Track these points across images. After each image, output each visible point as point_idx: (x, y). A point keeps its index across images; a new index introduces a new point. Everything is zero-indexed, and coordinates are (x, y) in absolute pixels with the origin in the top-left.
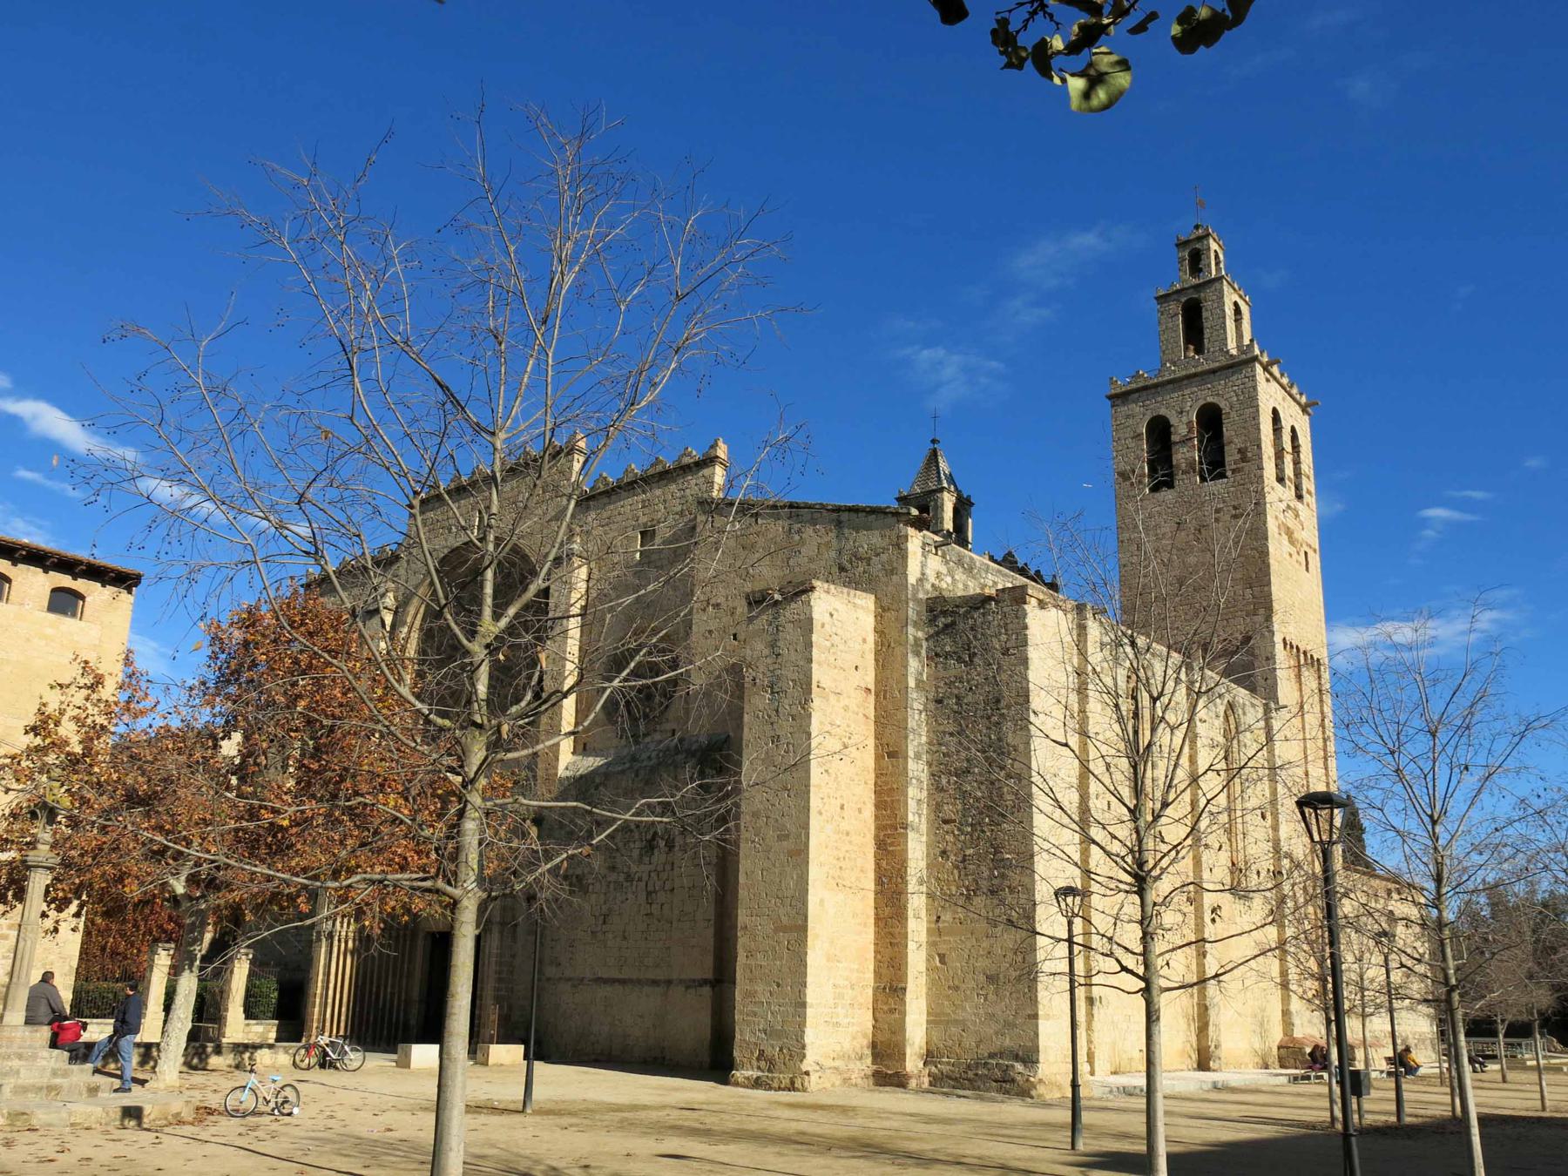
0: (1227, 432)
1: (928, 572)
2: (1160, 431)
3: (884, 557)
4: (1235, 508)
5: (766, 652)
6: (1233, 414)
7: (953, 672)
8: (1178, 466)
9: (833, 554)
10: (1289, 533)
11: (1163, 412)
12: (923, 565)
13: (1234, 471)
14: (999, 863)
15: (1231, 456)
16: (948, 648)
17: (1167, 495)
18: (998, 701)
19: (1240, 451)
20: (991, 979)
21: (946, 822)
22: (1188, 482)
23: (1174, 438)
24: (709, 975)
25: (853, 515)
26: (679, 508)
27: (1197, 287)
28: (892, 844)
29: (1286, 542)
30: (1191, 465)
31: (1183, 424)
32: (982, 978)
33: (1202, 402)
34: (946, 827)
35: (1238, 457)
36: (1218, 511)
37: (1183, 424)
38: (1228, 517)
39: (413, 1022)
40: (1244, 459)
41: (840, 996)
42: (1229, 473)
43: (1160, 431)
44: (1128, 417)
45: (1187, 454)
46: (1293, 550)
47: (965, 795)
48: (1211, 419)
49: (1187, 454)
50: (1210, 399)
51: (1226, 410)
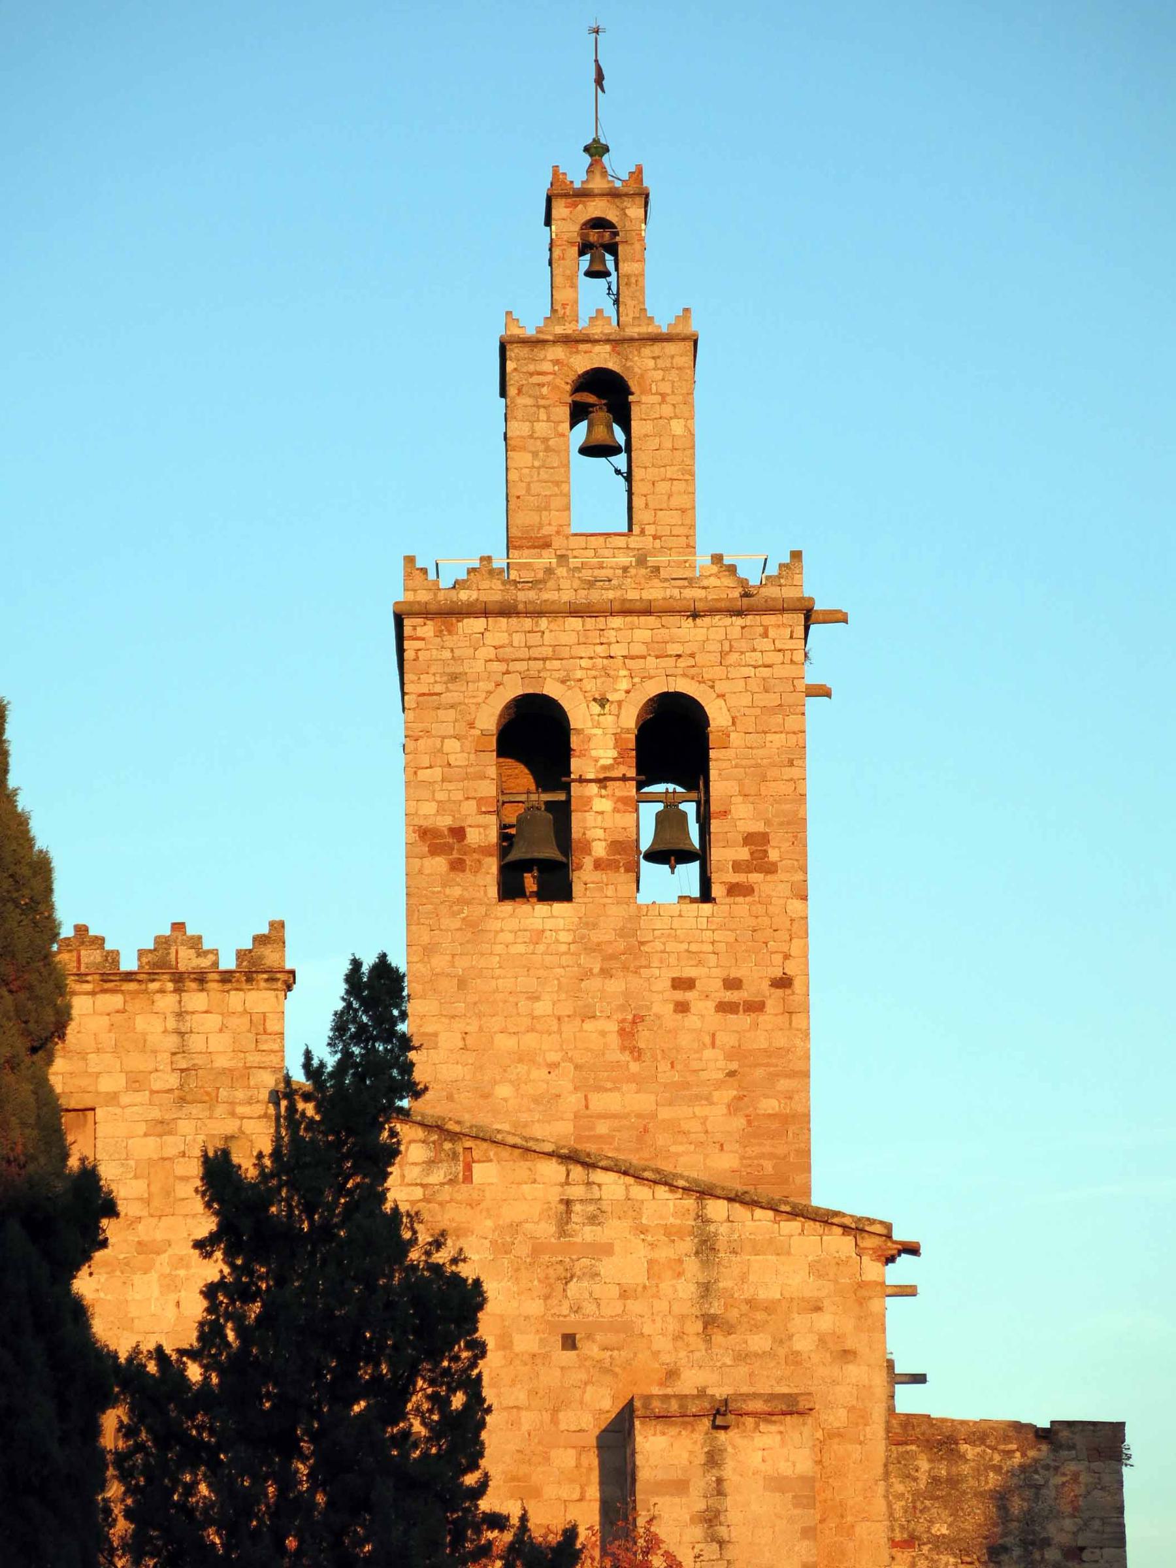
3: (825, 1322)
4: (732, 984)
5: (698, 1532)
8: (587, 848)
11: (552, 690)
16: (940, 1529)
19: (749, 839)
23: (575, 764)
25: (738, 1209)
26: (173, 1080)
31: (601, 739)
35: (743, 854)
36: (683, 984)
38: (711, 1005)
40: (760, 863)
43: (535, 734)
44: (454, 678)
48: (673, 741)
51: (717, 716)
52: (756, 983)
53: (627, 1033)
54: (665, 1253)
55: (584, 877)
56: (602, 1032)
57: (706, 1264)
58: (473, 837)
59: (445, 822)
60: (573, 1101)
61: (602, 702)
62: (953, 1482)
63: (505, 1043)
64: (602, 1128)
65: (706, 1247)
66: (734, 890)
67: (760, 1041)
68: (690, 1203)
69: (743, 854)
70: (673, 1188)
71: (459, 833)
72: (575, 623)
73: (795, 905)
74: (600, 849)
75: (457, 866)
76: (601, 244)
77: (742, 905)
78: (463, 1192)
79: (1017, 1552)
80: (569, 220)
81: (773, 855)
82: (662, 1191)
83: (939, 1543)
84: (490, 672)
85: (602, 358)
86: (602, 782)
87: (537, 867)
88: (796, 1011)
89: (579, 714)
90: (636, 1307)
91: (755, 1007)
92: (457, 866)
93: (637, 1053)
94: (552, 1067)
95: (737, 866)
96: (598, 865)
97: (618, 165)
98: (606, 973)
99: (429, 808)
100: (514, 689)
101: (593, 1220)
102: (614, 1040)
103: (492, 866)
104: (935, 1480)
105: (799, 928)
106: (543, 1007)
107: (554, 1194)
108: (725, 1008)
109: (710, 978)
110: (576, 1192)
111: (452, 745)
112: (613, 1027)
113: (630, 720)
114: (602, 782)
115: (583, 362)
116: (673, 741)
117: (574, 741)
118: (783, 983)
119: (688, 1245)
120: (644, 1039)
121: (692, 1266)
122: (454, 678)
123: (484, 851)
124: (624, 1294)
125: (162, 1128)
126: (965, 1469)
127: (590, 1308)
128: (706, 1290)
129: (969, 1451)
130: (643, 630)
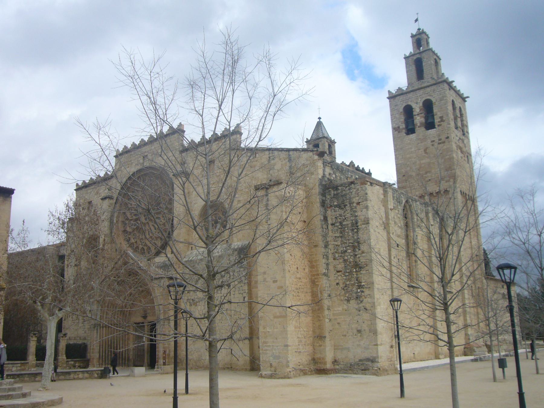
0: (435, 110)
1: (326, 173)
6: (437, 103)
7: (338, 213)
8: (417, 125)
9: (288, 168)
10: (461, 148)
11: (410, 103)
12: (324, 171)
13: (439, 126)
14: (360, 287)
15: (437, 120)
16: (335, 203)
17: (412, 136)
18: (357, 223)
20: (359, 331)
21: (338, 272)
22: (420, 131)
23: (414, 113)
24: (248, 336)
25: (295, 152)
27: (420, 53)
28: (317, 282)
29: (459, 153)
30: (421, 123)
31: (417, 108)
32: (355, 331)
33: (424, 99)
34: (339, 274)
36: (433, 141)
37: (417, 108)
39: (131, 357)
40: (442, 120)
41: (300, 341)
42: (436, 126)
44: (396, 105)
45: (419, 120)
46: (462, 155)
47: (345, 261)
48: (428, 106)
49: (419, 120)
50: (428, 98)
51: (434, 100)
53: (425, 151)
54: (284, 162)
55: (417, 129)
56: (421, 152)
57: (290, 163)
58: (401, 127)
59: (397, 126)
60: (418, 162)
61: (417, 103)
62: (337, 194)
63: (408, 156)
64: (423, 165)
65: (290, 160)
66: (439, 126)
67: (445, 147)
68: (287, 153)
69: (440, 120)
70: (285, 151)
71: (399, 127)
72: (412, 93)
73: (448, 126)
74: (419, 125)
75: (399, 132)
77: (440, 128)
78: (256, 159)
79: (349, 205)
81: (444, 119)
82: (283, 152)
83: (336, 206)
85: (418, 56)
86: (418, 115)
87: (410, 130)
89: (414, 106)
90: (280, 173)
91: (444, 142)
92: (399, 132)
93: (426, 153)
94: (415, 158)
95: (439, 122)
96: (419, 127)
98: (422, 143)
99: (394, 125)
100: (404, 105)
101: (273, 159)
102: (423, 152)
103: (404, 131)
104: (334, 194)
106: (413, 150)
107: (267, 156)
108: (439, 144)
109: (436, 140)
110: (271, 155)
111: (397, 115)
112: (423, 150)
113: (421, 104)
114: (418, 115)
115: (415, 58)
116: (428, 106)
117: (414, 110)
118: (448, 138)
119: (287, 160)
120: (428, 151)
121: (288, 163)
122: (396, 105)
123: (403, 129)
124: (278, 171)
126: (339, 191)
127: (273, 175)
128: (290, 167)
129: (340, 188)
130: (421, 91)
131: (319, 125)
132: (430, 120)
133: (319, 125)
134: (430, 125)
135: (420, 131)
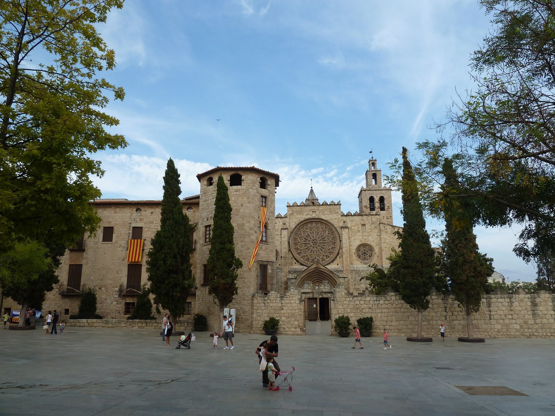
0: (386, 202)
2: (372, 199)
15: (386, 207)
22: (377, 210)
31: (377, 199)
37: (377, 199)
43: (372, 199)
45: (377, 205)
48: (382, 199)
49: (377, 205)
52: (389, 216)
76: (373, 164)
80: (371, 162)
84: (368, 195)
85: (375, 172)
88: (392, 219)
89: (375, 197)
97: (374, 159)
105: (392, 213)
116: (382, 199)
125: (371, 226)
130: (380, 191)
131: (312, 191)
132: (382, 206)
133: (312, 191)
134: (382, 209)
135: (377, 210)
